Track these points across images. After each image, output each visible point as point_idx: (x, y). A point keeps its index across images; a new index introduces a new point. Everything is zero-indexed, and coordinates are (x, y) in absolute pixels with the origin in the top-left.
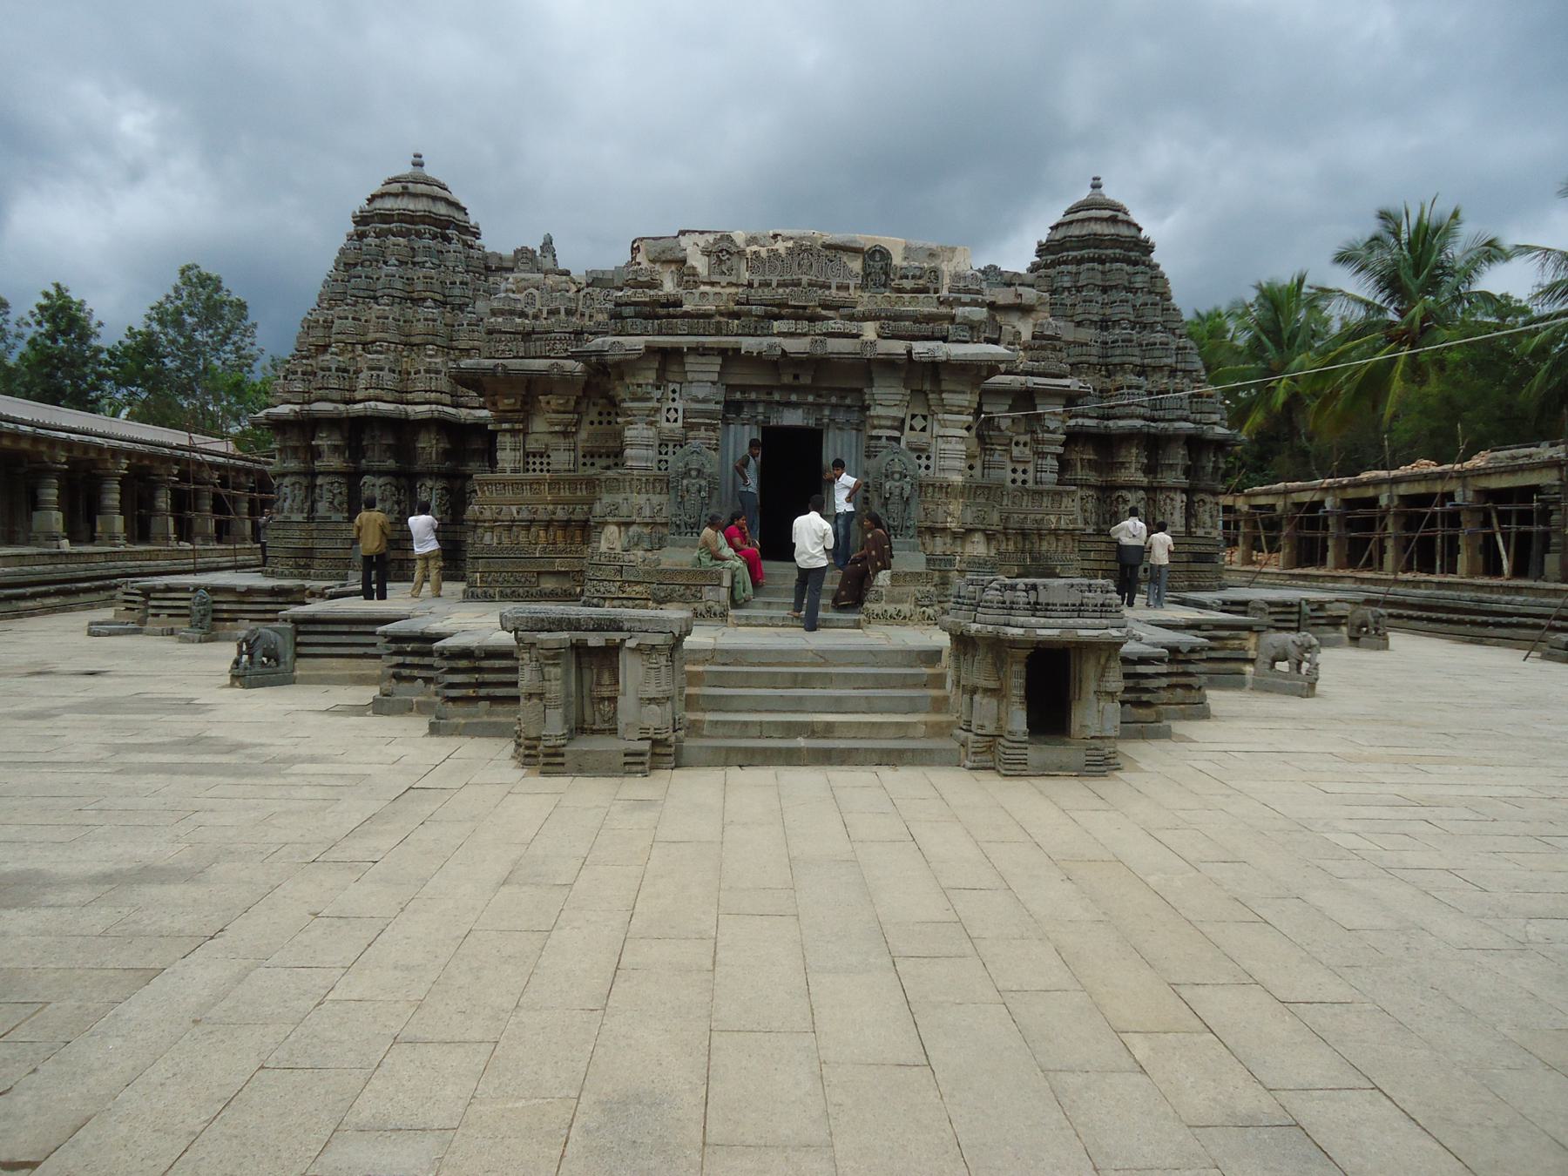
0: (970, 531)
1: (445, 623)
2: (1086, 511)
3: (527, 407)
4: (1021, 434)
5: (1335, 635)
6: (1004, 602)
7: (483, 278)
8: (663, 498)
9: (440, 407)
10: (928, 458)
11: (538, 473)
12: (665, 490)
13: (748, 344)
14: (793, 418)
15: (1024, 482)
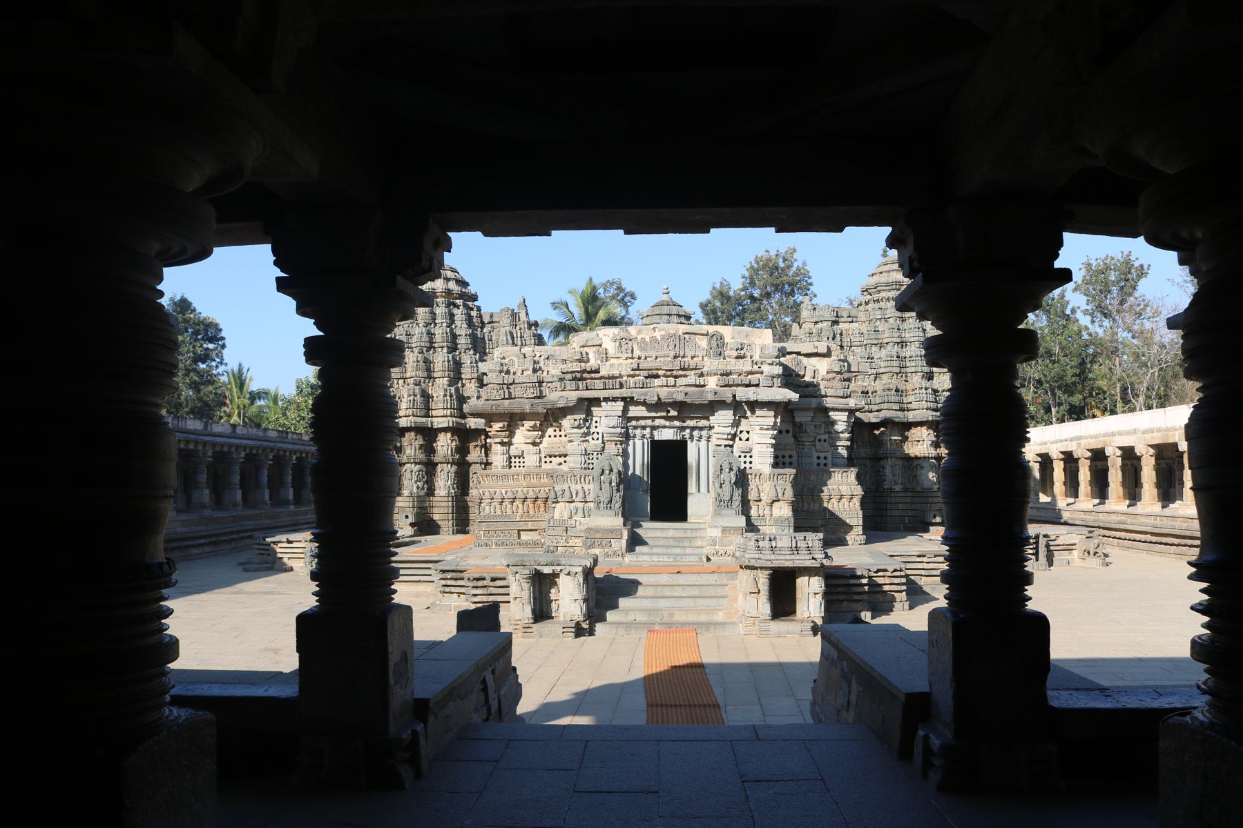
0: (774, 501)
1: (467, 562)
2: (894, 475)
3: (511, 428)
4: (822, 434)
5: (1069, 557)
6: (759, 547)
7: (479, 329)
8: (591, 486)
9: (454, 419)
10: (751, 457)
11: (517, 468)
12: (591, 481)
13: (637, 394)
14: (667, 435)
15: (825, 465)
